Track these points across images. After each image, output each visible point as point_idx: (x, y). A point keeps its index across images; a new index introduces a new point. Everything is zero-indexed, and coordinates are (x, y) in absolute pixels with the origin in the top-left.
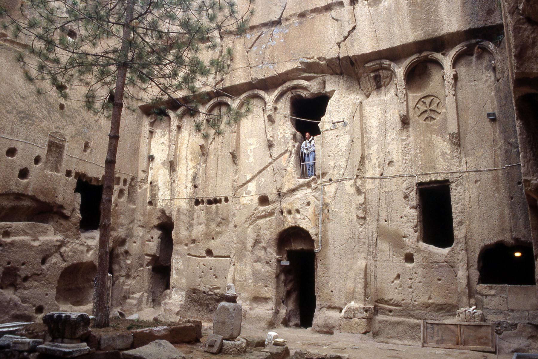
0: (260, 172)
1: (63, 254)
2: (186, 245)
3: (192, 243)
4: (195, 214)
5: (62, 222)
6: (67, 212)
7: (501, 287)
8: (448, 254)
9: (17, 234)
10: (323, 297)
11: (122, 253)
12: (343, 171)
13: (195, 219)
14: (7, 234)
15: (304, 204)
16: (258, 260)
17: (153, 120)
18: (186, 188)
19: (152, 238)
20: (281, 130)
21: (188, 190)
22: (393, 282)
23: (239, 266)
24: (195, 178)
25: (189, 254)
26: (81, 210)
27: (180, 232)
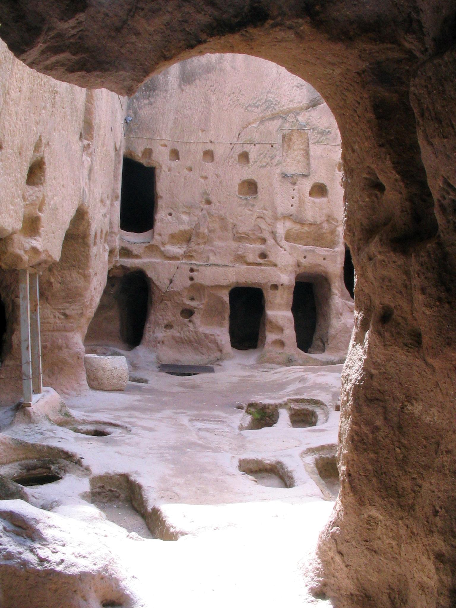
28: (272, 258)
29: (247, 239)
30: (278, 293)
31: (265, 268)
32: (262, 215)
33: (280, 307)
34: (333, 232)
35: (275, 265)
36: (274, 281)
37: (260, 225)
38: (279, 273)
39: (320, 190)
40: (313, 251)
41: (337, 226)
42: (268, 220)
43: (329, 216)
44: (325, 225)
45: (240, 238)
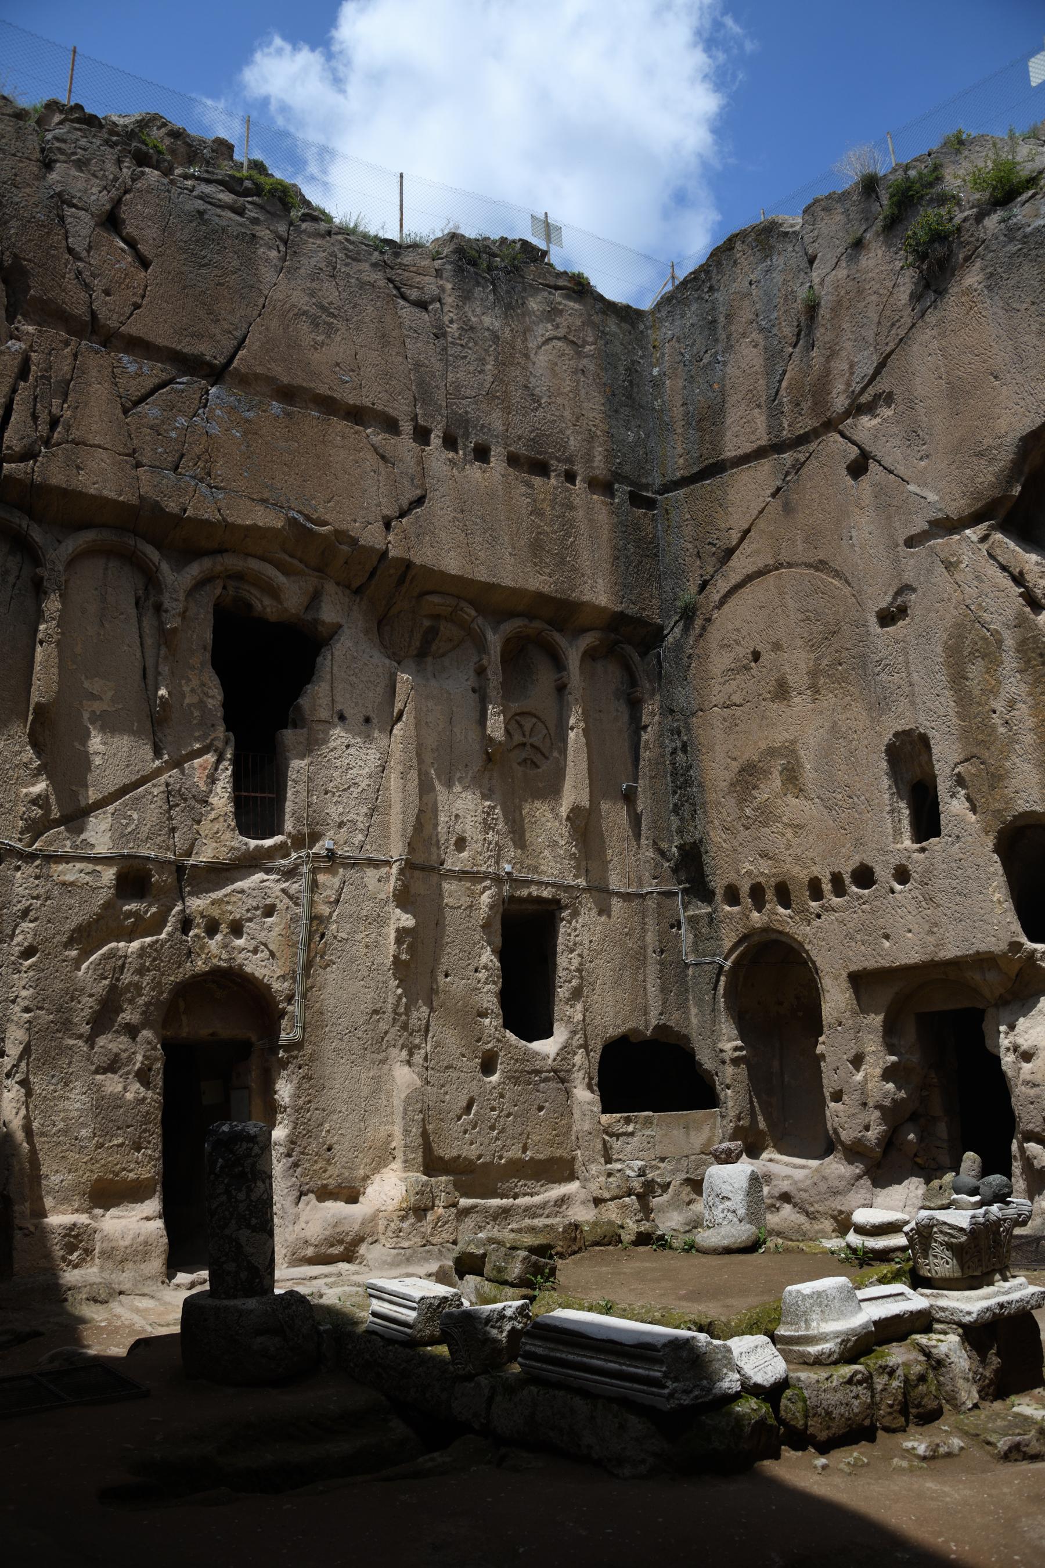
0: (124, 790)
7: (646, 1117)
8: (558, 1054)
10: (307, 1165)
12: (360, 837)
15: (257, 908)
22: (459, 1119)
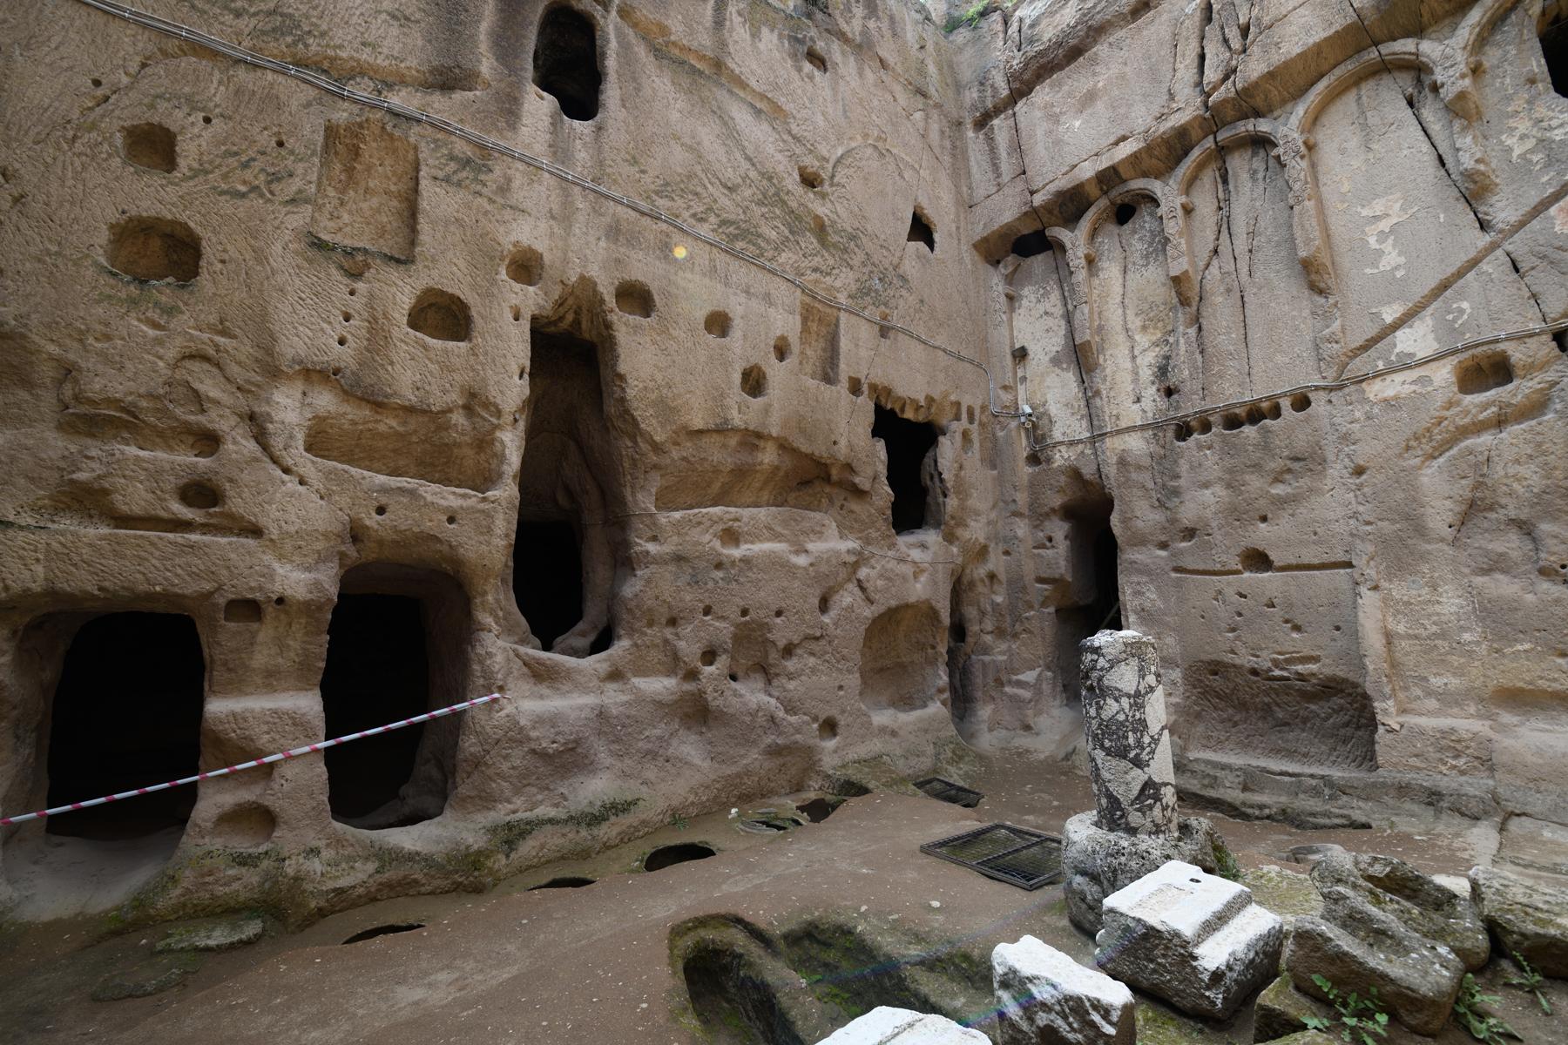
0: (1444, 286)
1: (866, 585)
2: (1163, 546)
3: (1184, 539)
4: (1182, 461)
5: (855, 506)
6: (862, 481)
9: (755, 537)
11: (982, 580)
13: (1184, 474)
14: (731, 536)
16: (1495, 565)
17: (1010, 269)
18: (1138, 400)
19: (1050, 539)
20: (1523, 126)
21: (1147, 404)
23: (1399, 590)
24: (1163, 371)
25: (1177, 570)
26: (888, 478)
27: (1134, 515)
28: (238, 503)
29: (127, 425)
30: (265, 632)
31: (207, 538)
32: (211, 352)
33: (271, 680)
34: (485, 442)
35: (256, 532)
36: (245, 586)
37: (196, 385)
38: (268, 558)
39: (445, 316)
40: (412, 493)
41: (496, 427)
42: (234, 370)
43: (473, 395)
44: (458, 418)
45: (93, 421)
